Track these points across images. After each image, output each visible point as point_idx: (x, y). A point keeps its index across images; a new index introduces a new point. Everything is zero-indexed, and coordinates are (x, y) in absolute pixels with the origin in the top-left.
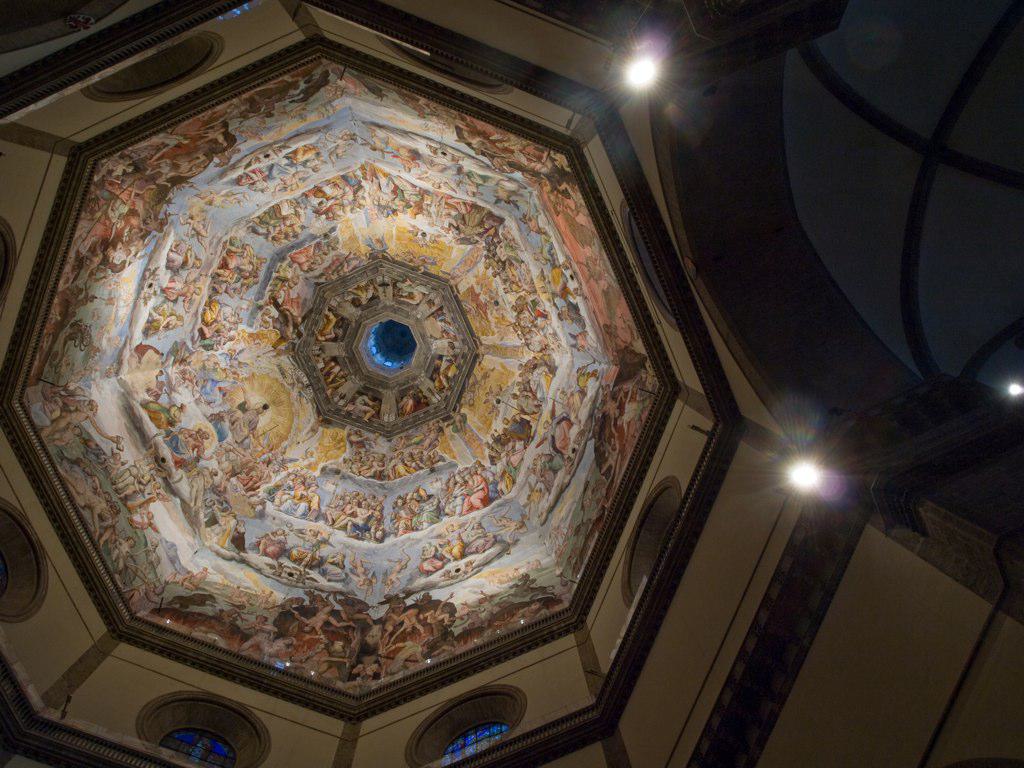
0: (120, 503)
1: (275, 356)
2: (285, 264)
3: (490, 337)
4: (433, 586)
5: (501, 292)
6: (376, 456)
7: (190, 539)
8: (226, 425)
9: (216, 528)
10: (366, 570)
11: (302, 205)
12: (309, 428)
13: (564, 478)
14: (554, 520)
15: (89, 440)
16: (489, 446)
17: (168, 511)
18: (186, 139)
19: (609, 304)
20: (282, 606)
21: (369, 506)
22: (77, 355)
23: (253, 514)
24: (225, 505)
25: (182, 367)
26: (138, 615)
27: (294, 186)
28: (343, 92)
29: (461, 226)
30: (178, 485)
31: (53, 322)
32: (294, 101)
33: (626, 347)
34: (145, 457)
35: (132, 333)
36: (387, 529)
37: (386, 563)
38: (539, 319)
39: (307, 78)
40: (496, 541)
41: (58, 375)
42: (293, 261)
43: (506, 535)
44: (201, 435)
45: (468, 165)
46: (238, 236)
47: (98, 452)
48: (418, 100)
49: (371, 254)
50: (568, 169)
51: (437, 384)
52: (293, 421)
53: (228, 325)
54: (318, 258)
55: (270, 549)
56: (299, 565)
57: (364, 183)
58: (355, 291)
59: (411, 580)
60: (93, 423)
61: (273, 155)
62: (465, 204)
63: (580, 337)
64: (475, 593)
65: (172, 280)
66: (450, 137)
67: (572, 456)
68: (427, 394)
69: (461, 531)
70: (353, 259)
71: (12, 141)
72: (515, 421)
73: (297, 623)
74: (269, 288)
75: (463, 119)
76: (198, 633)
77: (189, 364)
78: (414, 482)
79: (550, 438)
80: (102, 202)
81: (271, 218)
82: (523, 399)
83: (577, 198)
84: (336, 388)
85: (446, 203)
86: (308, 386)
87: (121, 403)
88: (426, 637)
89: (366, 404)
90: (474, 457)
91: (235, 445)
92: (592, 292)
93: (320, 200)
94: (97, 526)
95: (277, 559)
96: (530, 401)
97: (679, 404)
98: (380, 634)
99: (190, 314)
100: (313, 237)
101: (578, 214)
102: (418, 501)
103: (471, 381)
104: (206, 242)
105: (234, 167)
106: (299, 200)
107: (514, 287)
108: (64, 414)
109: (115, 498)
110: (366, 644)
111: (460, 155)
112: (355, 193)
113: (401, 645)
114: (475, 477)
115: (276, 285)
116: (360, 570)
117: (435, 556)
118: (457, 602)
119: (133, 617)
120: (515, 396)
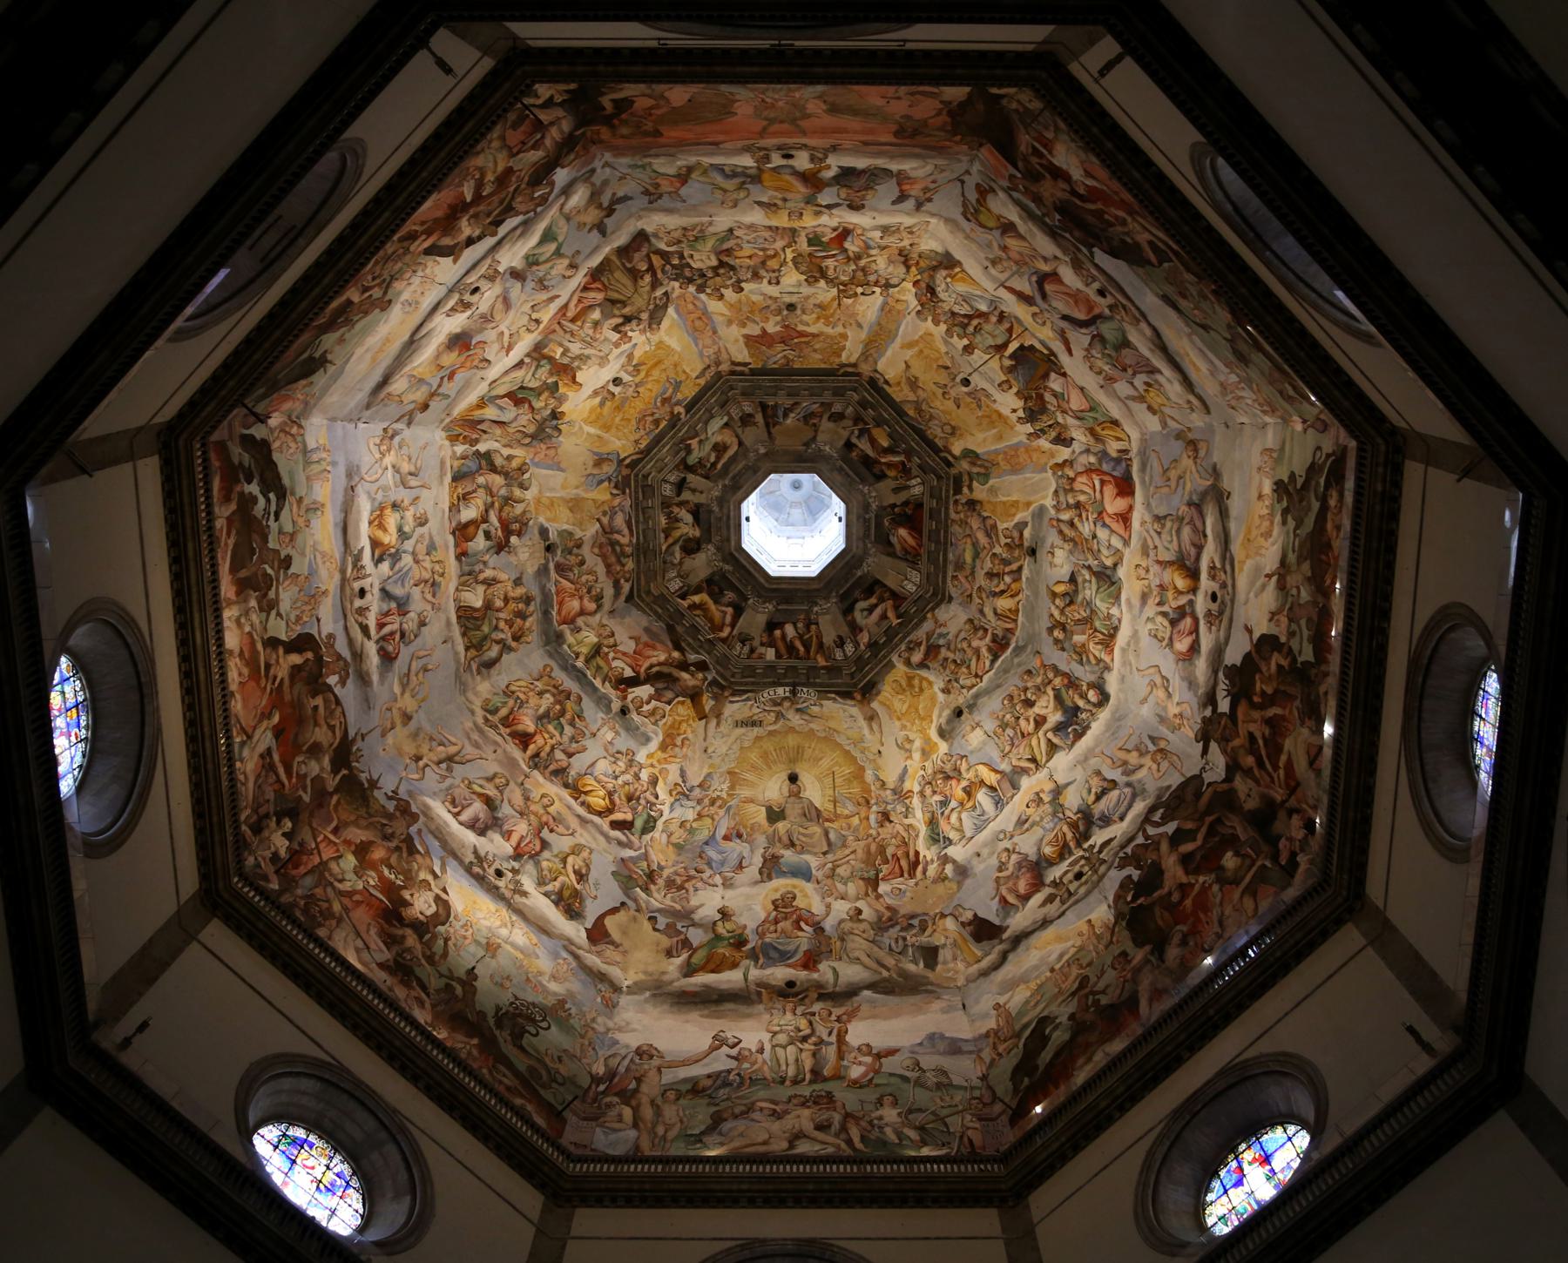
0: (817, 1087)
1: (718, 724)
2: (570, 639)
3: (848, 344)
4: (1218, 652)
5: (773, 291)
6: (963, 635)
7: (937, 1005)
8: (788, 856)
9: (944, 955)
10: (1137, 749)
11: (477, 568)
12: (863, 723)
13: (1142, 333)
14: (1209, 388)
15: (696, 1083)
16: (1035, 435)
17: (874, 1017)
18: (269, 716)
19: (854, 112)
20: (1119, 916)
21: (1039, 690)
22: (553, 1038)
23: (955, 887)
24: (915, 922)
25: (661, 882)
26: (1002, 1149)
27: (437, 567)
28: (295, 421)
29: (627, 311)
30: (843, 980)
31: (475, 1052)
32: (277, 519)
33: (950, 113)
34: (769, 1010)
35: (562, 937)
36: (1092, 678)
37: (1146, 711)
38: (847, 245)
39: (241, 476)
40: (1197, 506)
41: (570, 1081)
42: (570, 621)
43: (1196, 482)
44: (783, 906)
45: (511, 257)
46: (485, 695)
47: (721, 1079)
48: (349, 302)
49: (616, 487)
50: (573, 86)
51: (892, 473)
52: (839, 745)
53: (628, 777)
54: (584, 578)
55: (1022, 887)
56: (1071, 853)
57: (482, 447)
58: (670, 540)
59: (1191, 683)
60: (673, 1065)
61: (366, 583)
62: (585, 289)
63: (905, 187)
64: (1264, 587)
65: (507, 835)
66: (445, 270)
67: (1109, 300)
68: (900, 498)
69: (1152, 553)
70: (611, 518)
71: (141, 994)
72: (1011, 370)
73: (1157, 911)
74: (597, 683)
75: (412, 237)
76: (1080, 1078)
77: (661, 868)
78: (1036, 594)
79: (1064, 324)
80: (318, 891)
81: (478, 628)
82: (978, 338)
83: (629, 90)
84: (821, 645)
85: (573, 321)
86: (794, 693)
87: (666, 1007)
88: (1293, 710)
89: (871, 610)
90: (1043, 470)
91: (830, 857)
92: (824, 132)
93: (481, 533)
94: (830, 1139)
95: (1043, 884)
96: (987, 327)
97: (1075, 68)
98: (1249, 781)
99: (579, 830)
100: (543, 571)
101: (668, 101)
102: (1071, 602)
103: (911, 413)
104: (469, 750)
105: (358, 656)
106: (467, 569)
107: (773, 264)
108: (634, 1103)
109: (805, 1090)
110: (1249, 811)
111: (488, 261)
112: (493, 469)
113: (1284, 758)
114: (1077, 486)
115: (599, 668)
116: (1133, 758)
117: (1173, 623)
118: (1262, 627)
119: (1004, 1158)
120: (968, 349)
